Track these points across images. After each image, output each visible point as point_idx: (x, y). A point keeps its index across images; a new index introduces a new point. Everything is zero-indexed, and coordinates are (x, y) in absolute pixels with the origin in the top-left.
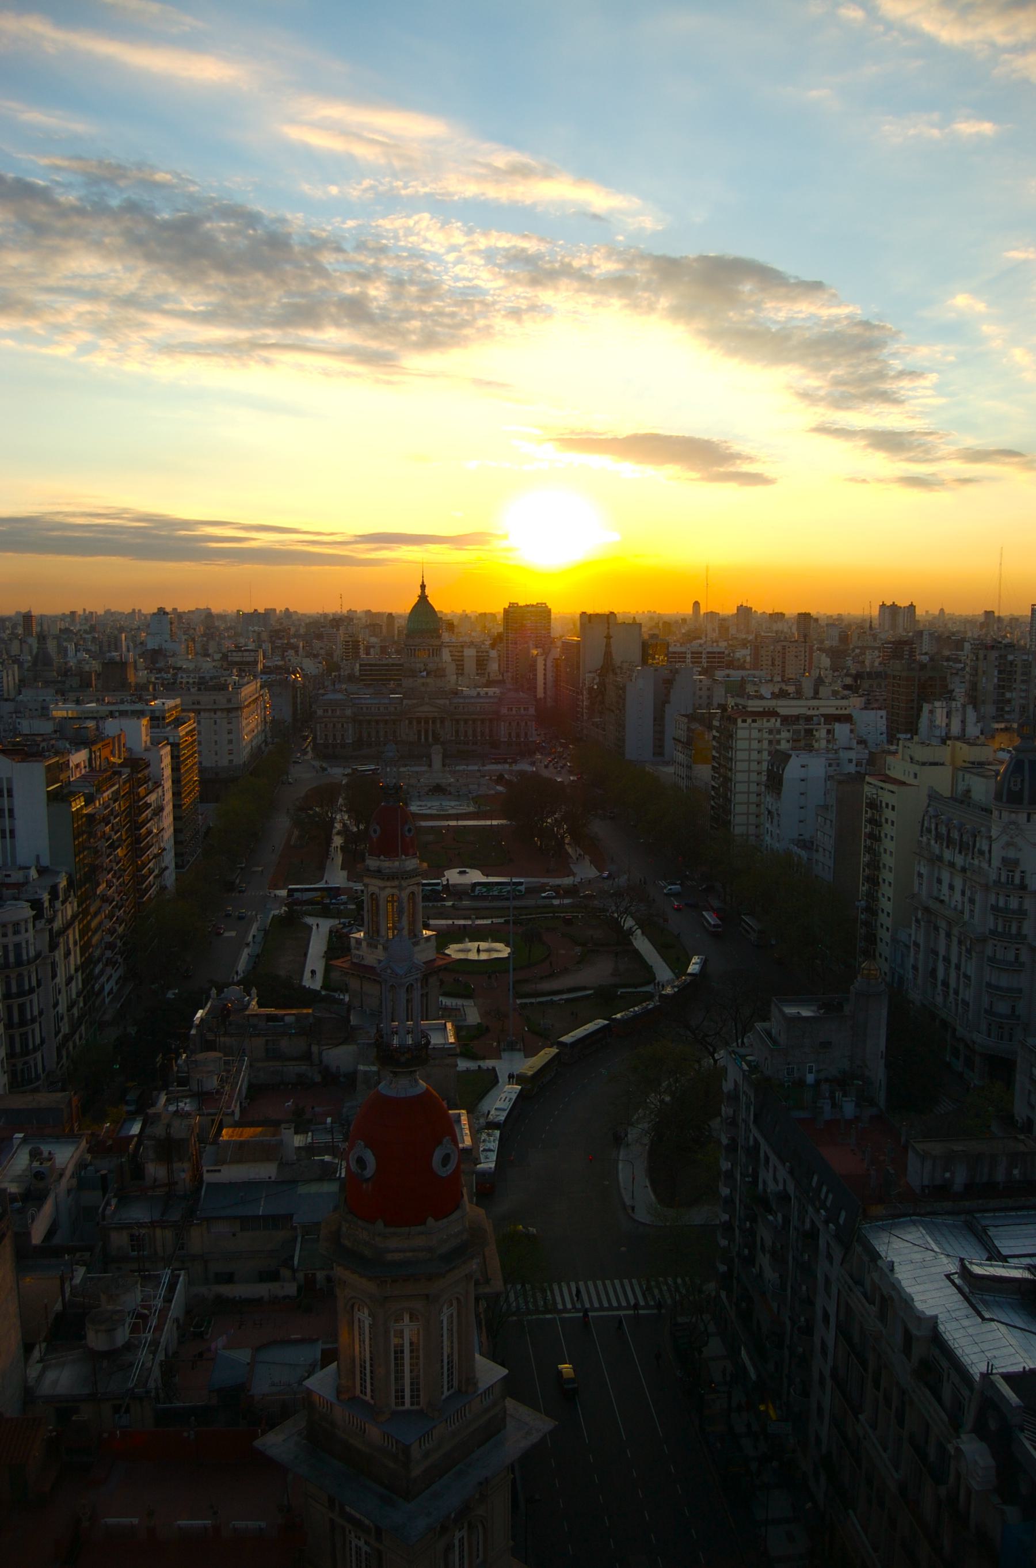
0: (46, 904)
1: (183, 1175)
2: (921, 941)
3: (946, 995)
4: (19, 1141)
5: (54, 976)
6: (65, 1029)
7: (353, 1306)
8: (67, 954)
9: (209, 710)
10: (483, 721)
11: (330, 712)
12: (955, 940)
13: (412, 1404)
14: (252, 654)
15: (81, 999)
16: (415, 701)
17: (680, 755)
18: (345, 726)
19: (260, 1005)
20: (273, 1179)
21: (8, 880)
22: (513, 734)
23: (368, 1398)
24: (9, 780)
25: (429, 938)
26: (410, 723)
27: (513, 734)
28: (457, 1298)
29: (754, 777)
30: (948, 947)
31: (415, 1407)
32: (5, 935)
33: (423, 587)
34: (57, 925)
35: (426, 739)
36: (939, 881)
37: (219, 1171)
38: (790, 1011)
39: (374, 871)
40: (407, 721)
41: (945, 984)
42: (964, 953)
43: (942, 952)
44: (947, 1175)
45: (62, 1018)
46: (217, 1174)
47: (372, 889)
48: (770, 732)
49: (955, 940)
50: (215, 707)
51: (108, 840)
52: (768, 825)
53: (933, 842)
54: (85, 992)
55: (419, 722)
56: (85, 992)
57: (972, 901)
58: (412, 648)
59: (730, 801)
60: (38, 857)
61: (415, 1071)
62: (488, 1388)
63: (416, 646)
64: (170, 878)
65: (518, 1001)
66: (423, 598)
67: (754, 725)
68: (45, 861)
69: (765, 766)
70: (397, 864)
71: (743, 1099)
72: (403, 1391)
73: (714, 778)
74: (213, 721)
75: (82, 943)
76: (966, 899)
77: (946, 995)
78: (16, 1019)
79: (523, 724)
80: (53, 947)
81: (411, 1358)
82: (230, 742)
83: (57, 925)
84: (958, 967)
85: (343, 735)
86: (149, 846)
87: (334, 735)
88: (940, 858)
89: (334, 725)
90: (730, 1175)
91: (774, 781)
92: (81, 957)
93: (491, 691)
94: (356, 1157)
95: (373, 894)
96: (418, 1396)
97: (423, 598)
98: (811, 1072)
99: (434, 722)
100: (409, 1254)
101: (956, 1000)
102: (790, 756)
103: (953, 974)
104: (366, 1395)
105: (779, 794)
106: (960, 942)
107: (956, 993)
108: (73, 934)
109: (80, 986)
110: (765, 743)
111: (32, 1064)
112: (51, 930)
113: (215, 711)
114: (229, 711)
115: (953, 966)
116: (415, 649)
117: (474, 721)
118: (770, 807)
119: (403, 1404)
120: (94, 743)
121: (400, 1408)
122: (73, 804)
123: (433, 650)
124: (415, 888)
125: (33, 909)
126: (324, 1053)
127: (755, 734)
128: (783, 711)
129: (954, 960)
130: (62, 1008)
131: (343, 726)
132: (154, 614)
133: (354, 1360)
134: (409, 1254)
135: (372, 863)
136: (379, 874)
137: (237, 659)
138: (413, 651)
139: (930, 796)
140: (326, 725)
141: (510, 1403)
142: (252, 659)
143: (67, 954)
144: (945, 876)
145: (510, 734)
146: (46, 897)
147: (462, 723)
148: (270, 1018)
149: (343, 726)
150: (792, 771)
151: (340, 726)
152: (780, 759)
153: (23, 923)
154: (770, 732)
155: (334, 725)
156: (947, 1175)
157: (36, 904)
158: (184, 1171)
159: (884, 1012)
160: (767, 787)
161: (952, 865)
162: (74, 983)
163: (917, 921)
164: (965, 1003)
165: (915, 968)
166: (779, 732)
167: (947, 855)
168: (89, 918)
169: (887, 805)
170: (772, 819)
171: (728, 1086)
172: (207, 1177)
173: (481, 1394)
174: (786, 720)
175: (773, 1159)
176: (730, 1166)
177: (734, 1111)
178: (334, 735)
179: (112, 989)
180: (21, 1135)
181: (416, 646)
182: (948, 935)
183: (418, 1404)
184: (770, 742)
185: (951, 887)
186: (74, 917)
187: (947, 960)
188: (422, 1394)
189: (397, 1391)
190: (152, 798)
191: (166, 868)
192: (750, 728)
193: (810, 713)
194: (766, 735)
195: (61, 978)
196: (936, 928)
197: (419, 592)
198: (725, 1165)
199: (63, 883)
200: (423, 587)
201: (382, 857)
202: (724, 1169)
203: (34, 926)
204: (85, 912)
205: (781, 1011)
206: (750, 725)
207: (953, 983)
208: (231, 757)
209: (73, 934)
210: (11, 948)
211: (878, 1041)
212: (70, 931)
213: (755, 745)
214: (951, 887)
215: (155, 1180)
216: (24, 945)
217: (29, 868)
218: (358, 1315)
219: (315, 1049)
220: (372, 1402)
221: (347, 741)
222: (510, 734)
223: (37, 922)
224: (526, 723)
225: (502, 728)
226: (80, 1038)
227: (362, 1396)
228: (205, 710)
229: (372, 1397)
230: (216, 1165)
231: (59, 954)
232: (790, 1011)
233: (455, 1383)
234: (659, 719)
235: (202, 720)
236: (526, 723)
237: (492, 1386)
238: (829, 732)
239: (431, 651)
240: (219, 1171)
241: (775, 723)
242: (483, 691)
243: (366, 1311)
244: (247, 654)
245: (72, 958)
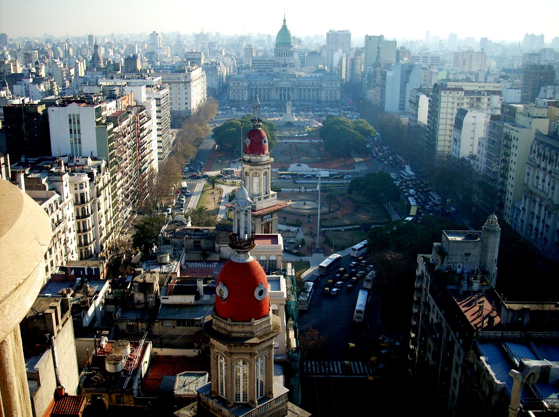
0: (95, 175)
1: (151, 300)
2: (527, 208)
3: (537, 235)
4: (79, 281)
5: (99, 209)
6: (105, 234)
7: (217, 356)
8: (106, 199)
9: (176, 82)
10: (313, 90)
11: (236, 84)
12: (543, 208)
13: (244, 400)
14: (199, 54)
15: (112, 221)
16: (279, 79)
17: (412, 109)
18: (244, 91)
19: (192, 224)
20: (192, 303)
21: (78, 163)
22: (329, 97)
23: (224, 397)
24: (78, 115)
25: (273, 196)
26: (277, 90)
27: (329, 97)
28: (266, 356)
29: (449, 122)
30: (540, 210)
31: (245, 402)
32: (76, 189)
33: (285, 21)
34: (100, 185)
35: (285, 98)
36: (538, 178)
37: (168, 298)
38: (451, 238)
39: (247, 162)
40: (275, 90)
41: (537, 229)
42: (547, 214)
43: (536, 213)
44: (520, 319)
45: (103, 229)
46: (166, 300)
47: (246, 170)
48: (458, 99)
49: (543, 208)
50: (179, 81)
51: (125, 145)
52: (454, 146)
53: (536, 157)
54: (114, 217)
55: (281, 90)
56: (114, 217)
57: (553, 188)
59: (436, 134)
60: (92, 153)
61: (248, 251)
62: (279, 397)
64: (155, 165)
65: (323, 229)
67: (450, 95)
68: (95, 155)
69: (454, 116)
70: (259, 158)
71: (425, 279)
72: (239, 395)
73: (428, 122)
74: (178, 88)
75: (113, 194)
76: (550, 187)
77: (537, 235)
78: (82, 228)
79: (333, 92)
80: (98, 195)
81: (244, 381)
82: (186, 98)
83: (100, 185)
84: (543, 221)
85: (243, 96)
86: (144, 149)
87: (238, 96)
88: (539, 166)
89: (238, 91)
90: (417, 315)
91: (458, 124)
92: (112, 201)
93: (318, 75)
94: (219, 289)
95: (246, 172)
96: (246, 398)
98: (459, 267)
99: (288, 90)
100: (242, 334)
101: (541, 238)
102: (467, 111)
103: (541, 224)
104: (223, 395)
105: (461, 131)
106: (546, 209)
107: (542, 234)
108: (108, 189)
109: (112, 215)
110: (456, 104)
111: (90, 249)
112: (97, 188)
113: (179, 83)
114: (186, 83)
115: (541, 221)
117: (309, 90)
118: (456, 138)
119: (239, 400)
120: (119, 98)
121: (238, 402)
122: (108, 127)
124: (267, 170)
125: (89, 177)
126: (221, 248)
127: (450, 100)
128: (466, 88)
129: (542, 217)
130: (103, 224)
132: (151, 34)
133: (218, 380)
134: (242, 334)
135: (247, 157)
136: (249, 162)
137: (191, 57)
139: (536, 134)
140: (234, 91)
141: (290, 405)
142: (198, 57)
143: (106, 199)
144: (541, 176)
145: (327, 97)
146: (95, 171)
147: (303, 91)
148: (196, 230)
150: (468, 119)
151: (241, 91)
152: (462, 113)
153: (84, 184)
154: (458, 99)
155: (238, 91)
156: (520, 319)
157: (91, 175)
158: (152, 298)
159: (498, 240)
160: (455, 127)
161: (545, 169)
162: (108, 213)
163: (525, 197)
164: (546, 239)
165: (522, 221)
166: (463, 99)
167: (543, 165)
168: (116, 182)
169: (514, 137)
170: (456, 143)
171: (418, 273)
172: (163, 301)
173: (276, 399)
174: (467, 93)
175: (437, 308)
176: (417, 311)
177: (421, 285)
178: (238, 96)
179: (127, 216)
180: (80, 279)
182: (540, 205)
183: (246, 400)
184: (458, 104)
185: (544, 181)
186: (109, 182)
187: (538, 217)
188: (248, 396)
189: (236, 395)
190: (145, 126)
191: (154, 159)
192: (448, 96)
193: (480, 89)
194: (456, 101)
195: (102, 211)
196: (535, 201)
197: (282, 23)
198: (415, 310)
199: (103, 165)
200: (285, 21)
201: (251, 155)
202: (414, 312)
203: (90, 185)
204: (114, 179)
205: (447, 237)
206: (448, 95)
207: (540, 229)
208: (187, 106)
209: (108, 189)
210: (79, 195)
211: (494, 254)
212: (107, 188)
213: (450, 105)
214: (544, 181)
215: (139, 301)
216: (85, 194)
217: (88, 158)
218: (220, 360)
219: (217, 245)
220: (225, 398)
221: (245, 99)
222: (327, 97)
223: (91, 183)
224: (335, 91)
225: (323, 94)
226: (112, 239)
227: (222, 396)
228: (174, 82)
229: (226, 396)
230: (166, 295)
231: (101, 199)
232: (451, 238)
233: (264, 394)
234: (403, 91)
235: (173, 88)
236: (335, 91)
237: (281, 396)
238: (489, 100)
240: (168, 298)
241: (461, 94)
242: (314, 75)
243: (223, 359)
244: (195, 54)
245: (108, 200)
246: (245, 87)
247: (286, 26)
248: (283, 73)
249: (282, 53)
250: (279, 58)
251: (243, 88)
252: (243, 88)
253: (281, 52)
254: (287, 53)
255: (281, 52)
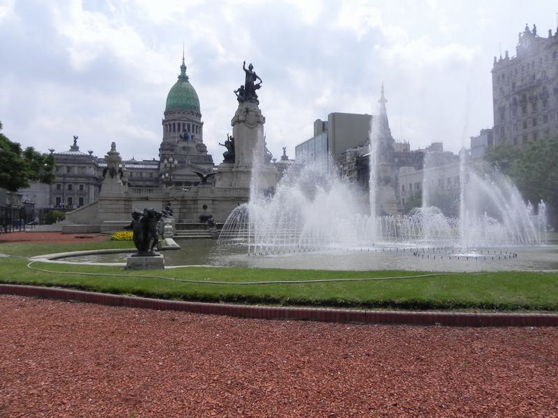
18: (85, 188)
33: (183, 68)
58: (172, 123)
63: (174, 120)
66: (183, 78)
97: (183, 78)
116: (174, 124)
123: (193, 126)
131: (81, 189)
138: (172, 126)
149: (81, 189)
151: (78, 187)
181: (174, 120)
197: (179, 73)
200: (183, 68)
239: (191, 126)
246: (88, 177)
247: (187, 78)
248: (183, 152)
249: (179, 125)
250: (172, 134)
251: (83, 180)
252: (83, 180)
253: (177, 122)
254: (189, 126)
255: (177, 122)
